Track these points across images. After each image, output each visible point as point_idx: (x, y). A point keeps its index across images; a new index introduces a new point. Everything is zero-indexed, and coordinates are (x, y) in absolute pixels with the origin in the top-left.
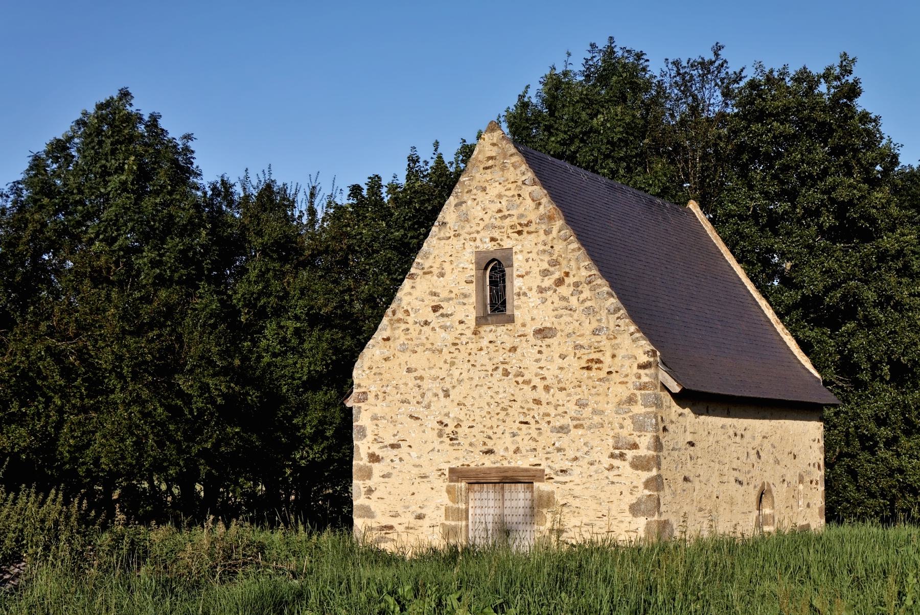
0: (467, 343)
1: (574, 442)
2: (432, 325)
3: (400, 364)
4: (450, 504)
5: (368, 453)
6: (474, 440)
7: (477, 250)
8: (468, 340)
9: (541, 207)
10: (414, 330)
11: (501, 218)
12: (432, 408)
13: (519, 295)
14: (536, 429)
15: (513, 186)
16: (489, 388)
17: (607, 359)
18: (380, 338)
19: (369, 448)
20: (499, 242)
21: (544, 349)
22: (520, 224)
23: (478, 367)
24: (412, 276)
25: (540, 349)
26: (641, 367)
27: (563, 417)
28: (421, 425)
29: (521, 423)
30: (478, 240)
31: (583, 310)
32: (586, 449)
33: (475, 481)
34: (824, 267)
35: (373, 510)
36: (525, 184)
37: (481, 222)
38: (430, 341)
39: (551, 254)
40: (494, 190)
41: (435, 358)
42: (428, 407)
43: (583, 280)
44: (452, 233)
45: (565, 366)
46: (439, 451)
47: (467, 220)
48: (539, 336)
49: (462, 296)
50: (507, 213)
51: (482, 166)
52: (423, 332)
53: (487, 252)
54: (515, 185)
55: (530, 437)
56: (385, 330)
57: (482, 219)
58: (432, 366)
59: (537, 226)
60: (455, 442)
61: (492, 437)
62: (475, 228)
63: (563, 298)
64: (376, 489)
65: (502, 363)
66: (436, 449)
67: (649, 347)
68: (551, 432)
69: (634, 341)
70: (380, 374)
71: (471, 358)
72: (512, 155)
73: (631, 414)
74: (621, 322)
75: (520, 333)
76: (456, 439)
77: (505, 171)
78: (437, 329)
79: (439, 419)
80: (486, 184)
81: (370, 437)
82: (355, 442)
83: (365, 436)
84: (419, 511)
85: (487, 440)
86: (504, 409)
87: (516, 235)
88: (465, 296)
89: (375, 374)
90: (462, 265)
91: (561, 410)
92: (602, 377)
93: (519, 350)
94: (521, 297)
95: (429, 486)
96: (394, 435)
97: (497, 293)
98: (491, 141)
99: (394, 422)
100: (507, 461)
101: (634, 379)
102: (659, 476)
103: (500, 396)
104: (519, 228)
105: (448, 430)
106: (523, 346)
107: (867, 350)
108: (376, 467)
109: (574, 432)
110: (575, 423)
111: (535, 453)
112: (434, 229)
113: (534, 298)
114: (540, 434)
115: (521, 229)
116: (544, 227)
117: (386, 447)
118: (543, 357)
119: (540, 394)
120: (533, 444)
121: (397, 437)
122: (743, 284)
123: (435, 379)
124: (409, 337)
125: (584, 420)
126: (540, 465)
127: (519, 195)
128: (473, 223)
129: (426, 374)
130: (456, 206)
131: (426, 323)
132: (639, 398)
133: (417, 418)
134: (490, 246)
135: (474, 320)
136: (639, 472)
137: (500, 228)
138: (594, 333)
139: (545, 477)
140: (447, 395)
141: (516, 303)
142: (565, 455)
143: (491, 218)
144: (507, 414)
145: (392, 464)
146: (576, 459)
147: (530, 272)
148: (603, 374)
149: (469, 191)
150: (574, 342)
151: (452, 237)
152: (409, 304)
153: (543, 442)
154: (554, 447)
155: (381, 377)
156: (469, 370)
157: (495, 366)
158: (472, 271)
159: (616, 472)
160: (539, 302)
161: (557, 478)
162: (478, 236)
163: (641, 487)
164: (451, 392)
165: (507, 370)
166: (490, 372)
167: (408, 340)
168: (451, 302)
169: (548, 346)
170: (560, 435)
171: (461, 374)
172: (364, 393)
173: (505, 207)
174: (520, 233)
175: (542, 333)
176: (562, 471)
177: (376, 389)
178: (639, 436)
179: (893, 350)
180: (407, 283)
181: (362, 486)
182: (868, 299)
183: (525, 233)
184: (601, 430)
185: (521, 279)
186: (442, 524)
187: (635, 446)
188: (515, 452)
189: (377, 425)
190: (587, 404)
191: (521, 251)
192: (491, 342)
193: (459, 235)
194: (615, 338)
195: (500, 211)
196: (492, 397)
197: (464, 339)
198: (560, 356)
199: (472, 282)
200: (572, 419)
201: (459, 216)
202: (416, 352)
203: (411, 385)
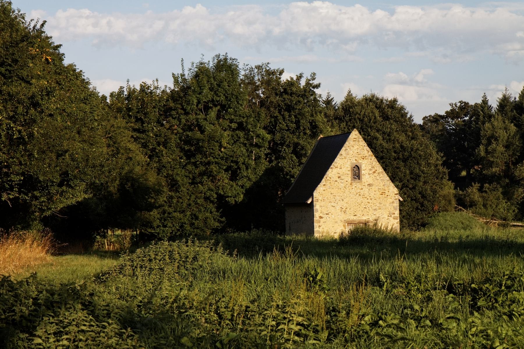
10: (333, 183)
17: (387, 192)
24: (332, 168)
26: (395, 194)
42: (337, 203)
53: (354, 163)
62: (351, 157)
63: (375, 176)
81: (319, 212)
99: (327, 208)
113: (367, 176)
118: (370, 191)
119: (369, 201)
120: (368, 214)
131: (336, 181)
140: (343, 200)
158: (349, 169)
159: (389, 220)
163: (396, 224)
174: (363, 159)
175: (369, 185)
180: (330, 170)
187: (394, 214)
195: (358, 153)
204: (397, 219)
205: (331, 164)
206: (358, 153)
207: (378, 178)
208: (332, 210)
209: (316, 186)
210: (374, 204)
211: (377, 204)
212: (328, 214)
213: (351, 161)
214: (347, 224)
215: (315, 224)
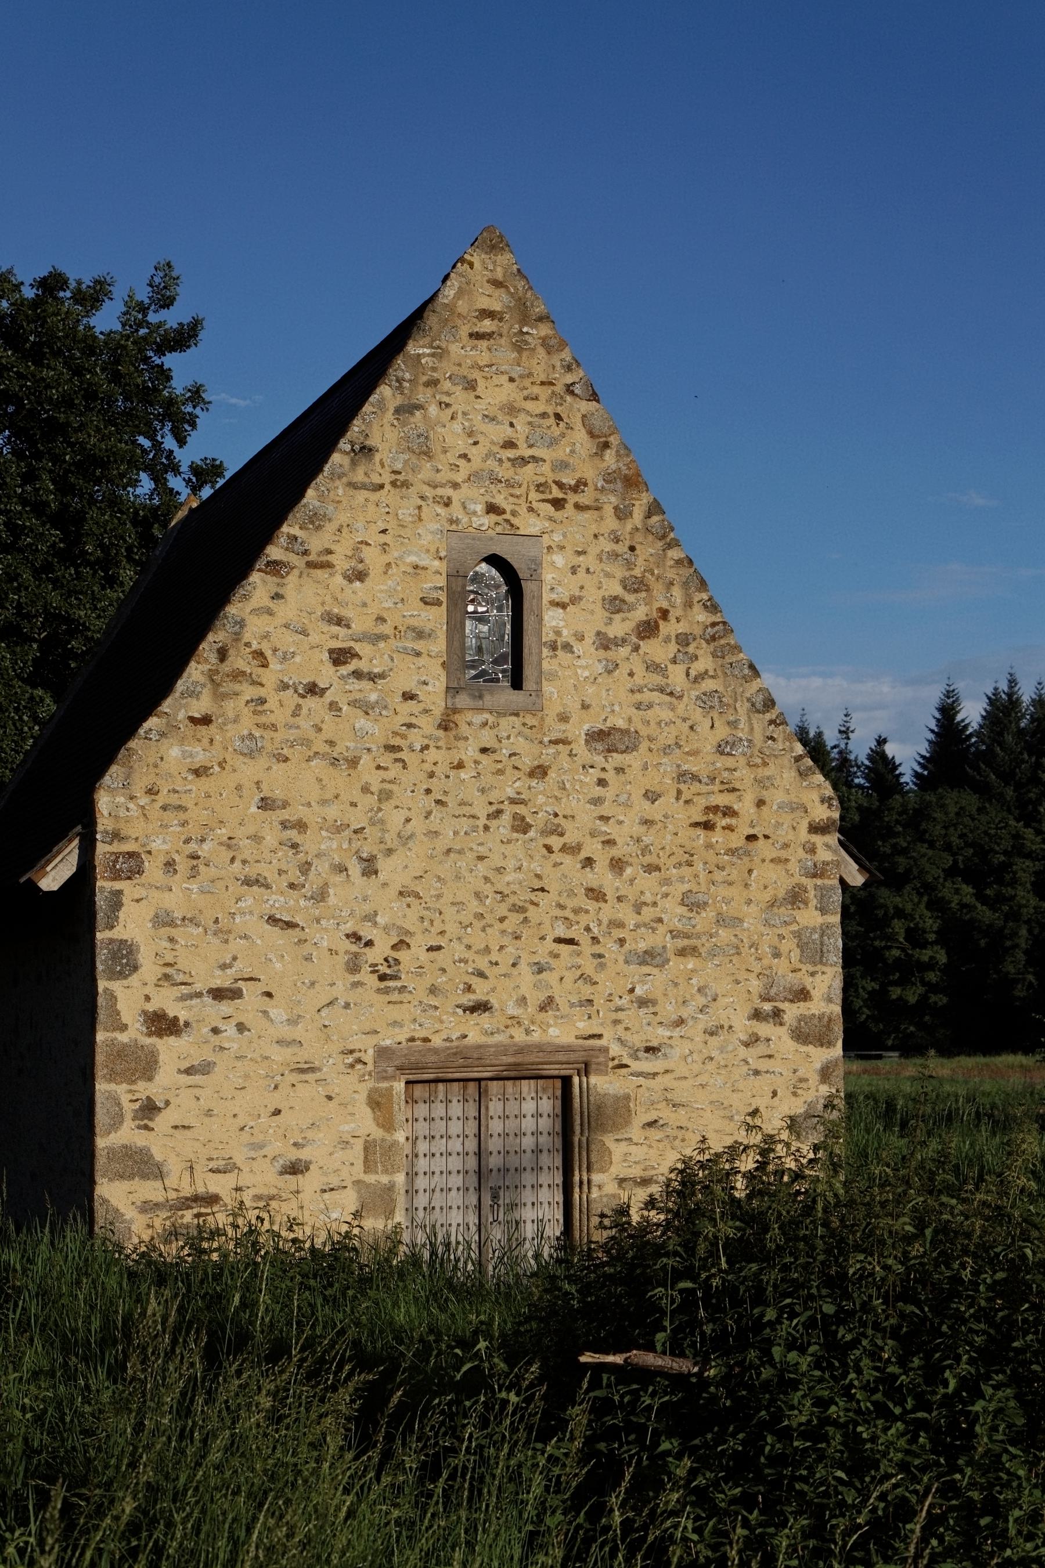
0: (426, 747)
1: (676, 985)
2: (329, 696)
3: (239, 788)
4: (378, 1133)
7: (454, 527)
8: (426, 742)
9: (609, 455)
12: (332, 900)
13: (554, 647)
14: (594, 956)
15: (544, 392)
16: (481, 858)
17: (745, 806)
18: (181, 715)
19: (148, 998)
20: (508, 516)
21: (610, 776)
22: (560, 485)
24: (275, 567)
25: (603, 775)
27: (654, 930)
28: (302, 942)
29: (559, 940)
31: (698, 698)
32: (701, 1001)
33: (432, 1076)
35: (158, 1157)
36: (572, 393)
37: (462, 463)
39: (630, 565)
41: (338, 780)
42: (320, 896)
43: (698, 631)
44: (387, 478)
45: (658, 817)
47: (428, 454)
48: (600, 746)
49: (411, 634)
50: (528, 453)
51: (464, 331)
54: (548, 390)
55: (579, 973)
56: (197, 696)
58: (329, 796)
60: (391, 984)
61: (488, 973)
62: (445, 475)
63: (653, 667)
64: (167, 1103)
65: (513, 801)
66: (342, 1002)
68: (627, 962)
70: (180, 808)
71: (434, 784)
73: (794, 927)
76: (395, 977)
77: (525, 354)
78: (345, 708)
79: (349, 927)
81: (149, 969)
82: (102, 985)
83: (135, 968)
84: (293, 1154)
85: (475, 981)
87: (549, 508)
88: (420, 634)
89: (164, 808)
90: (412, 559)
91: (648, 913)
92: (734, 846)
93: (552, 774)
94: (559, 652)
96: (224, 967)
99: (223, 934)
100: (522, 1029)
101: (801, 852)
103: (508, 878)
104: (556, 493)
105: (373, 956)
109: (677, 965)
110: (681, 943)
112: (336, 458)
114: (602, 966)
115: (561, 496)
117: (199, 995)
118: (609, 793)
119: (602, 876)
120: (587, 991)
121: (228, 971)
124: (263, 719)
126: (599, 1036)
127: (558, 417)
128: (442, 461)
130: (398, 411)
131: (313, 690)
132: (812, 893)
133: (290, 925)
136: (810, 1049)
137: (509, 484)
139: (611, 1064)
140: (370, 868)
141: (545, 665)
142: (655, 1014)
145: (215, 1040)
146: (680, 1022)
147: (580, 598)
149: (433, 383)
150: (679, 766)
151: (388, 487)
152: (266, 636)
153: (607, 983)
154: (633, 997)
155: (182, 816)
156: (428, 814)
157: (494, 808)
159: (761, 1049)
160: (600, 668)
161: (636, 1066)
162: (456, 496)
163: (814, 1079)
164: (381, 864)
165: (523, 818)
166: (482, 821)
167: (264, 727)
169: (620, 770)
170: (646, 969)
172: (131, 855)
174: (558, 504)
176: (648, 1050)
177: (165, 847)
181: (125, 1099)
183: (569, 506)
184: (735, 959)
186: (357, 1183)
187: (802, 995)
188: (543, 1008)
189: (171, 940)
190: (706, 903)
192: (484, 750)
193: (406, 484)
194: (765, 764)
195: (510, 444)
196: (486, 879)
197: (416, 739)
198: (646, 795)
199: (438, 603)
200: (674, 934)
202: (286, 760)
203: (270, 840)
204: (822, 1041)
205: (267, 536)
206: (510, 444)
207: (677, 676)
209: (130, 731)
210: (638, 908)
212: (235, 994)
213: (456, 511)
214: (399, 1086)
215: (102, 1087)
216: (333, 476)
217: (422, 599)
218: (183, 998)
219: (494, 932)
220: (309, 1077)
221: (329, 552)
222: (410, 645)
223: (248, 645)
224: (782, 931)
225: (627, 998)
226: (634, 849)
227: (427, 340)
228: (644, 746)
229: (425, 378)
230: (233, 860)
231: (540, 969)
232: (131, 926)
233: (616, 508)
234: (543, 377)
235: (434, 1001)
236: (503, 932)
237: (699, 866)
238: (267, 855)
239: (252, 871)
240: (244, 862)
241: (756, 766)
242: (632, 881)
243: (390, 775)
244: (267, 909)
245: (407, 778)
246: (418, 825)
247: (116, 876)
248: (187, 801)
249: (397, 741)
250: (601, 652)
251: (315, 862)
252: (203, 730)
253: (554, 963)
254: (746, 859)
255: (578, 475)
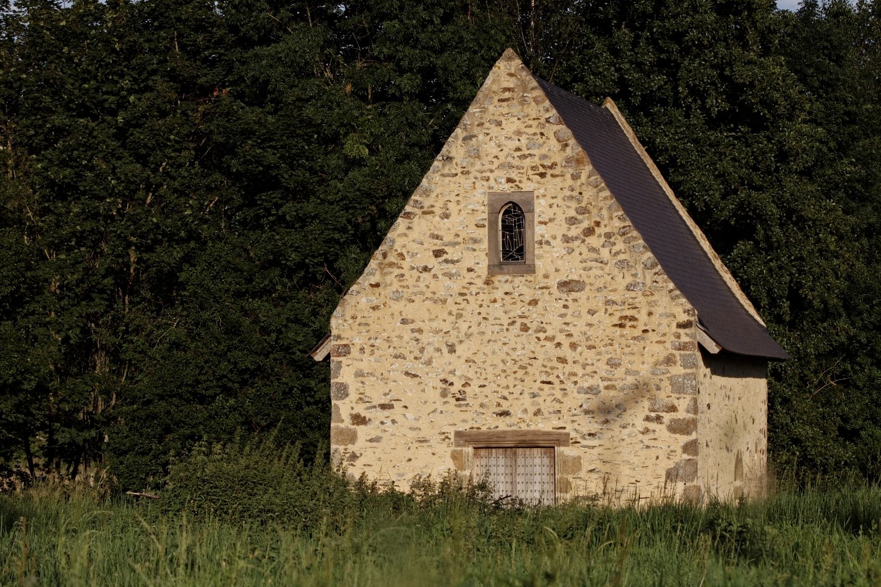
0: (478, 293)
3: (392, 315)
5: (351, 415)
6: (485, 401)
9: (568, 150)
10: (411, 277)
11: (520, 157)
12: (434, 364)
13: (541, 243)
14: (561, 389)
15: (536, 122)
16: (505, 344)
17: (642, 316)
18: (367, 284)
19: (352, 408)
20: (517, 183)
21: (570, 303)
22: (543, 166)
23: (491, 320)
24: (408, 215)
25: (566, 303)
26: (680, 326)
27: (592, 377)
28: (420, 383)
29: (543, 382)
30: (492, 180)
31: (616, 263)
33: (484, 446)
34: (716, 169)
37: (495, 160)
38: (431, 290)
39: (579, 201)
40: (511, 126)
41: (437, 309)
42: (429, 362)
43: (616, 231)
44: (459, 170)
45: (595, 322)
46: (441, 412)
47: (479, 157)
48: (565, 289)
49: (471, 241)
50: (527, 152)
51: (496, 98)
52: (422, 279)
54: (537, 122)
56: (374, 274)
57: (496, 157)
58: (433, 317)
59: (563, 169)
60: (462, 402)
62: (488, 166)
63: (593, 250)
64: (361, 454)
65: (520, 317)
67: (689, 306)
68: (578, 392)
69: (673, 299)
70: (367, 324)
72: (533, 89)
73: (669, 375)
74: (659, 278)
75: (541, 285)
76: (464, 400)
77: (525, 106)
78: (440, 277)
79: (442, 377)
80: (502, 119)
81: (353, 395)
82: (333, 402)
83: (347, 395)
85: (502, 401)
86: (522, 367)
87: (538, 177)
88: (475, 241)
89: (359, 325)
90: (471, 207)
91: (589, 369)
92: (636, 335)
93: (540, 303)
94: (544, 246)
95: (430, 451)
96: (385, 394)
97: (511, 237)
98: (509, 71)
99: (385, 380)
101: (673, 338)
102: (697, 439)
103: (518, 353)
104: (542, 170)
105: (454, 389)
106: (545, 298)
107: (768, 281)
108: (361, 430)
110: (606, 383)
111: (559, 415)
112: (436, 163)
114: (565, 395)
115: (544, 171)
116: (571, 171)
117: (375, 407)
118: (569, 312)
120: (557, 406)
121: (388, 397)
122: (674, 207)
123: (437, 332)
124: (403, 283)
125: (616, 380)
127: (542, 134)
128: (485, 160)
129: (425, 327)
130: (464, 139)
131: (426, 269)
132: (678, 358)
133: (415, 376)
134: (507, 187)
135: (486, 269)
136: (678, 436)
137: (518, 168)
138: (628, 288)
139: (571, 441)
140: (452, 349)
141: (536, 252)
143: (507, 156)
144: (526, 373)
145: (382, 427)
148: (637, 332)
149: (481, 125)
151: (459, 174)
152: (404, 246)
154: (582, 409)
155: (367, 328)
156: (480, 324)
157: (510, 321)
158: (483, 215)
159: (651, 436)
160: (564, 252)
161: (584, 442)
162: (492, 176)
163: (679, 451)
164: (459, 348)
166: (506, 326)
167: (404, 287)
168: (457, 247)
169: (575, 300)
171: (470, 327)
172: (345, 346)
173: (524, 146)
174: (542, 175)
175: (567, 286)
176: (590, 435)
178: (678, 399)
179: (800, 282)
180: (401, 223)
182: (773, 214)
183: (548, 176)
185: (544, 226)
187: (673, 409)
188: (535, 414)
191: (544, 196)
192: (506, 293)
193: (468, 173)
194: (652, 294)
195: (518, 149)
196: (508, 354)
198: (589, 312)
199: (484, 226)
201: (468, 151)
202: (413, 301)
207: (605, 253)
208: (406, 389)
210: (584, 366)
211: (599, 364)
212: (391, 407)
216: (434, 172)
217: (476, 225)
218: (368, 408)
219: (511, 379)
220: (424, 444)
221: (433, 206)
222: (470, 246)
223: (396, 250)
224: (662, 377)
225: (579, 409)
226: (583, 338)
227: (478, 105)
228: (588, 288)
229: (477, 123)
230: (389, 347)
231: (534, 396)
232: (345, 376)
233: (572, 175)
234: (534, 117)
235: (482, 410)
236: (516, 378)
237: (616, 346)
238: (405, 344)
239: (397, 352)
240: (394, 348)
241: (647, 295)
242: (581, 354)
243: (461, 307)
244: (404, 369)
245: (469, 308)
246: (475, 329)
247: (339, 355)
248: (370, 321)
249: (465, 291)
250: (565, 245)
251: (427, 347)
252: (376, 289)
253: (541, 393)
254: (642, 342)
255: (552, 161)
